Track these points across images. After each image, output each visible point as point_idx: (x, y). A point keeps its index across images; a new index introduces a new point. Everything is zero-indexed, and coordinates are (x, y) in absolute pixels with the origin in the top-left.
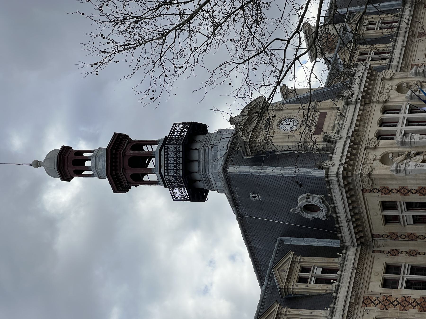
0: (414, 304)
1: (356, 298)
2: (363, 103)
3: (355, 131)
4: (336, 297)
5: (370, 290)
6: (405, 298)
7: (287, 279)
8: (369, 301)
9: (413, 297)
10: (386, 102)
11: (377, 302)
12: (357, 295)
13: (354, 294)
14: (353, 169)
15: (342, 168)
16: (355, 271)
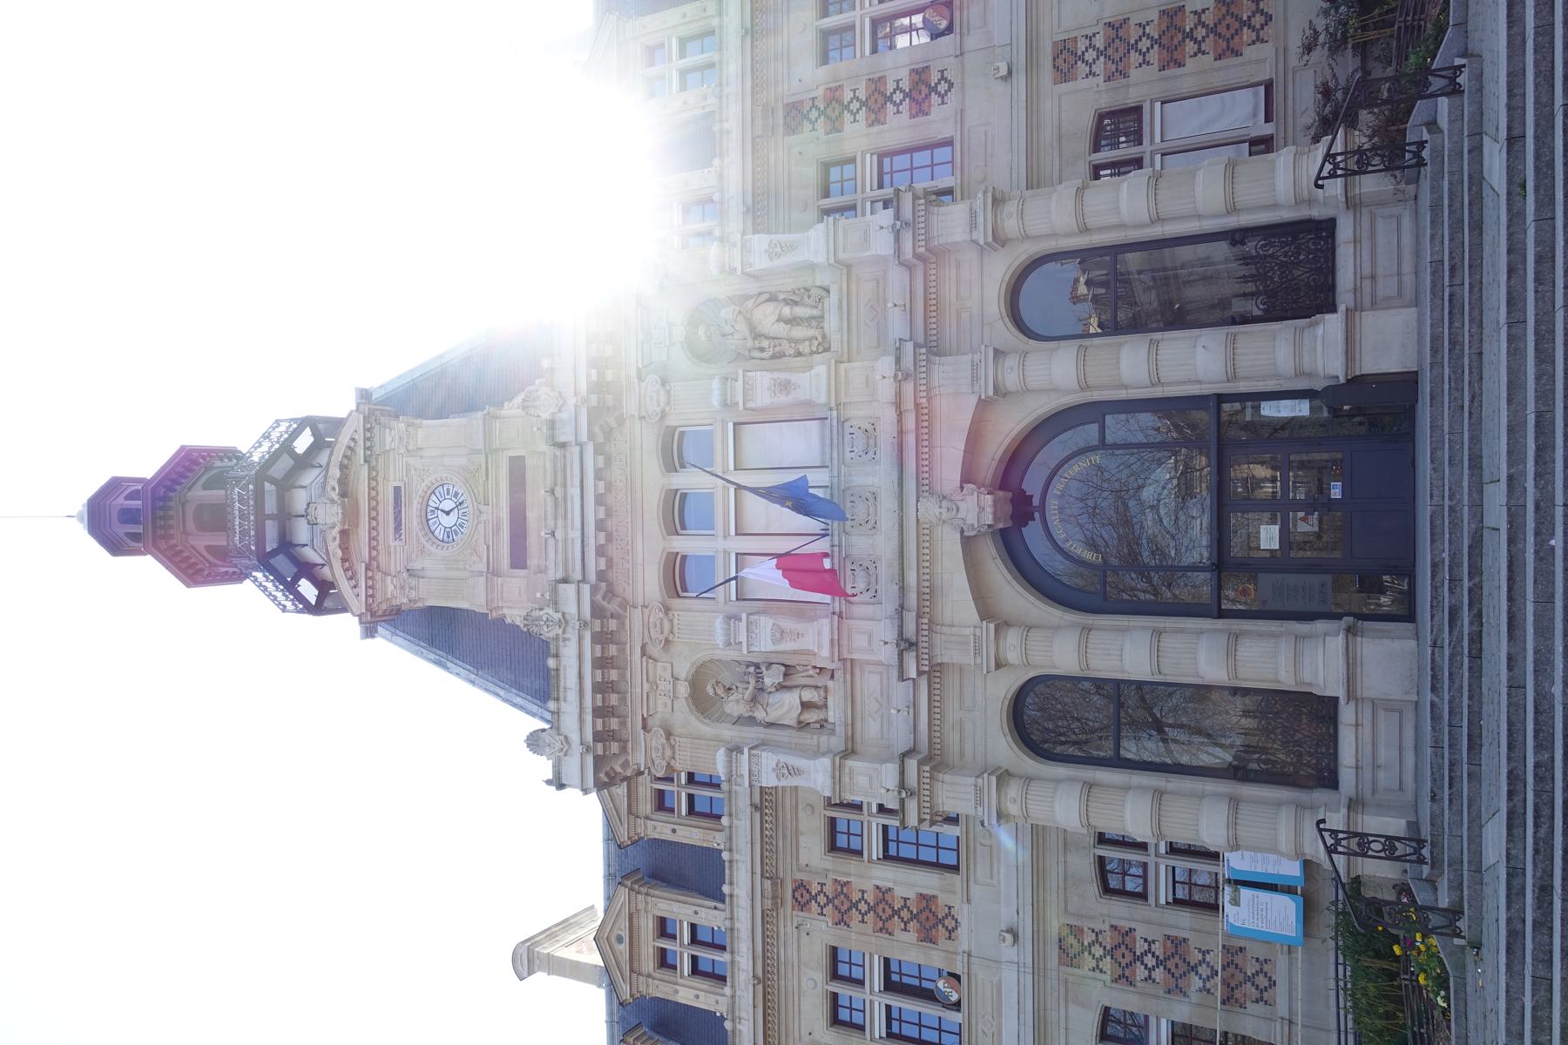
0: (905, 914)
1: (774, 891)
2: (601, 439)
3: (601, 576)
4: (731, 896)
5: (803, 862)
6: (883, 894)
7: (630, 813)
8: (807, 896)
9: (900, 892)
10: (663, 415)
11: (822, 899)
12: (774, 884)
13: (768, 883)
14: (624, 750)
15: (590, 760)
16: (757, 815)
